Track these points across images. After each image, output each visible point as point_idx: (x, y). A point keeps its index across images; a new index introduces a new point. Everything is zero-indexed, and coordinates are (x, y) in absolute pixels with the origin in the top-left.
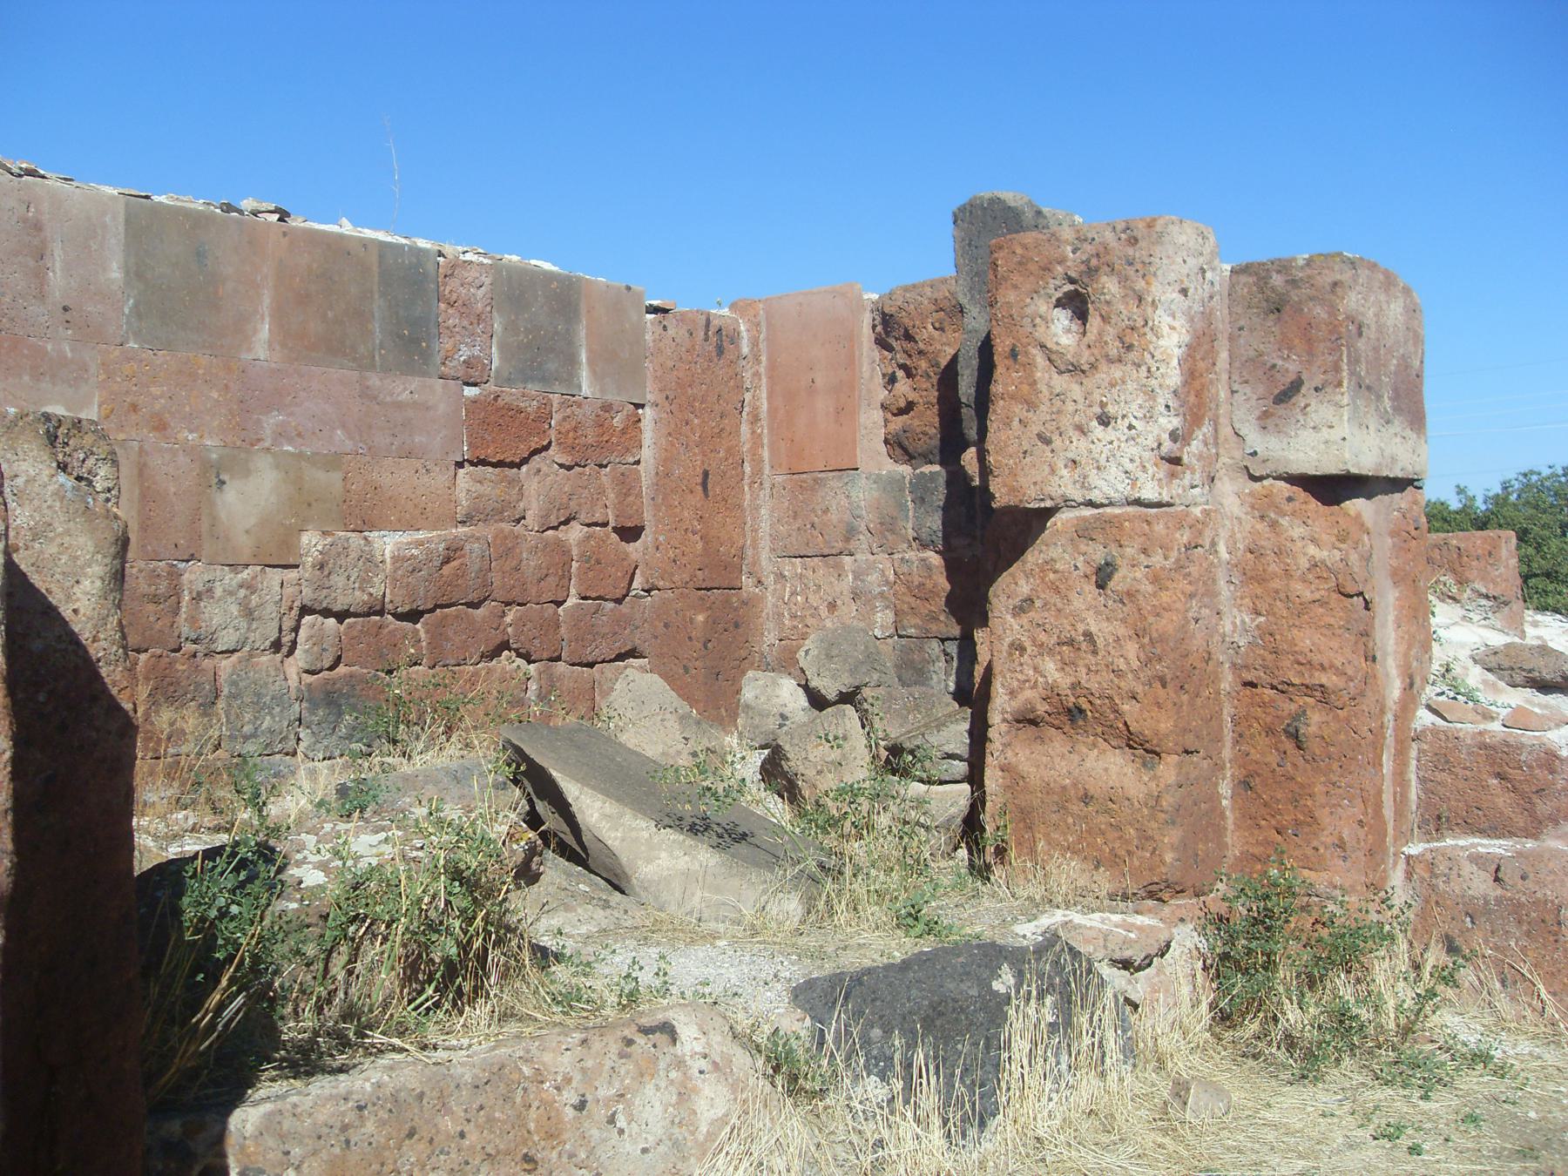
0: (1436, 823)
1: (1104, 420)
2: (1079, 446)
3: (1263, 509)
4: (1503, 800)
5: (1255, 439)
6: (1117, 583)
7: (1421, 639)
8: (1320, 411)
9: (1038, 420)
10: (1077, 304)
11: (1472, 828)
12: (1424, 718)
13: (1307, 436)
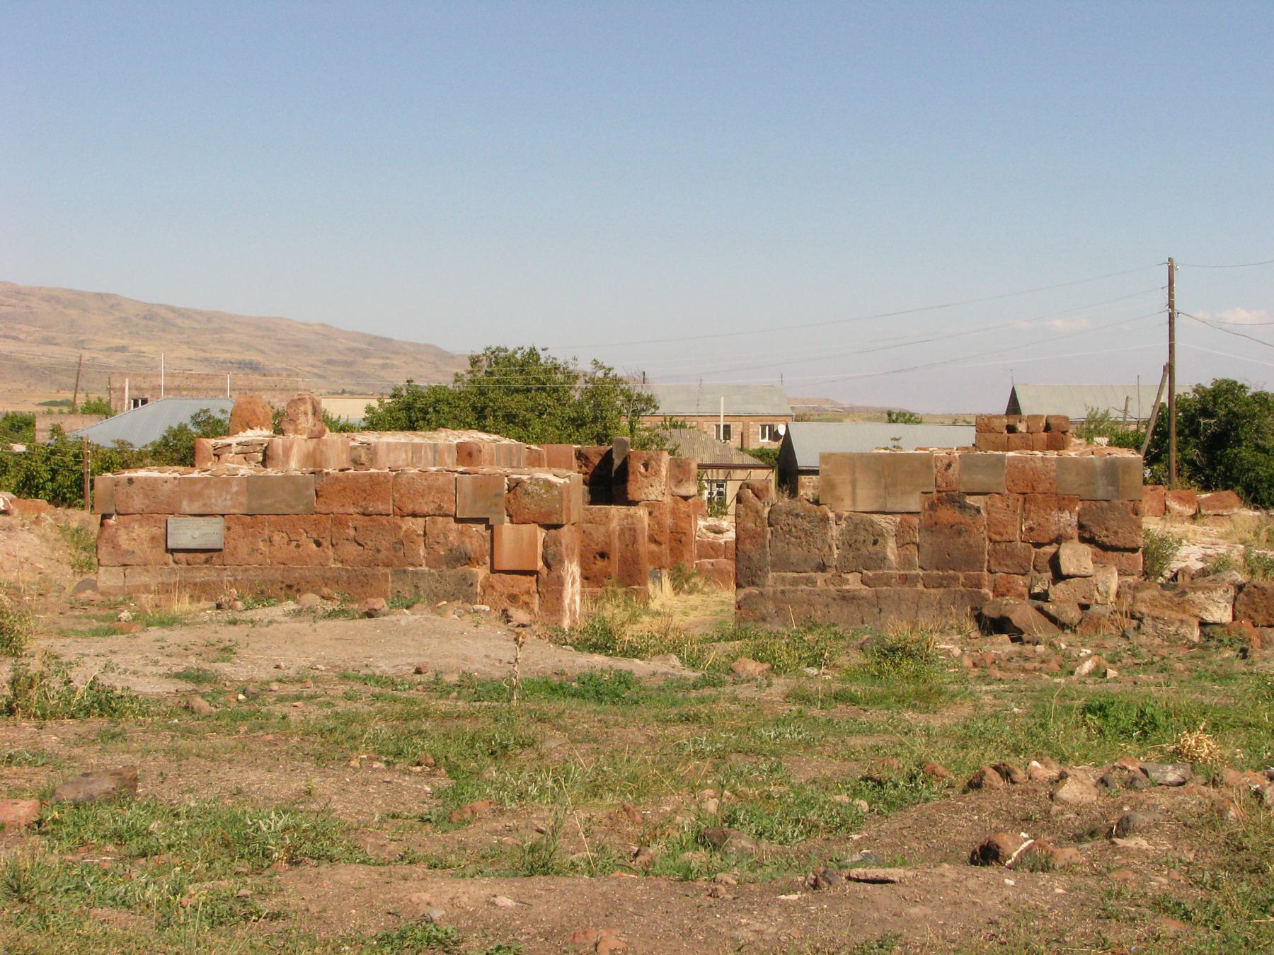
0: (700, 557)
1: (651, 486)
2: (646, 490)
3: (676, 502)
4: (712, 552)
5: (674, 489)
6: (654, 514)
7: (696, 524)
8: (686, 485)
9: (638, 485)
10: (646, 466)
11: (706, 558)
12: (697, 538)
13: (683, 489)
